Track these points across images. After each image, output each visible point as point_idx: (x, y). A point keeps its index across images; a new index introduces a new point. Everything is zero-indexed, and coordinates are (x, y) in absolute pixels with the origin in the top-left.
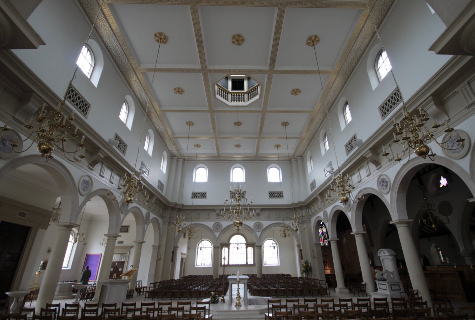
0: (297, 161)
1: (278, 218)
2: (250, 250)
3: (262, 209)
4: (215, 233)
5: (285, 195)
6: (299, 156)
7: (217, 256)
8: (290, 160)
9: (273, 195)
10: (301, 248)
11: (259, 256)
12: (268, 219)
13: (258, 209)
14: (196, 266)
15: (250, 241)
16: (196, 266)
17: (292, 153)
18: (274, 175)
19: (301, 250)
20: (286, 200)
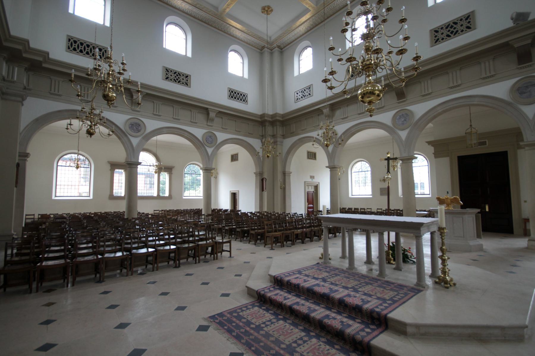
0: (272, 54)
1: (238, 132)
2: (165, 177)
3: (220, 112)
4: (132, 139)
5: (250, 99)
6: (279, 47)
7: (103, 183)
8: (261, 49)
9: (234, 95)
10: (265, 176)
11: (177, 185)
12: (224, 129)
13: (213, 111)
14: (54, 198)
15: (165, 163)
16: (54, 198)
17: (273, 38)
18: (237, 64)
19: (262, 180)
20: (252, 106)
